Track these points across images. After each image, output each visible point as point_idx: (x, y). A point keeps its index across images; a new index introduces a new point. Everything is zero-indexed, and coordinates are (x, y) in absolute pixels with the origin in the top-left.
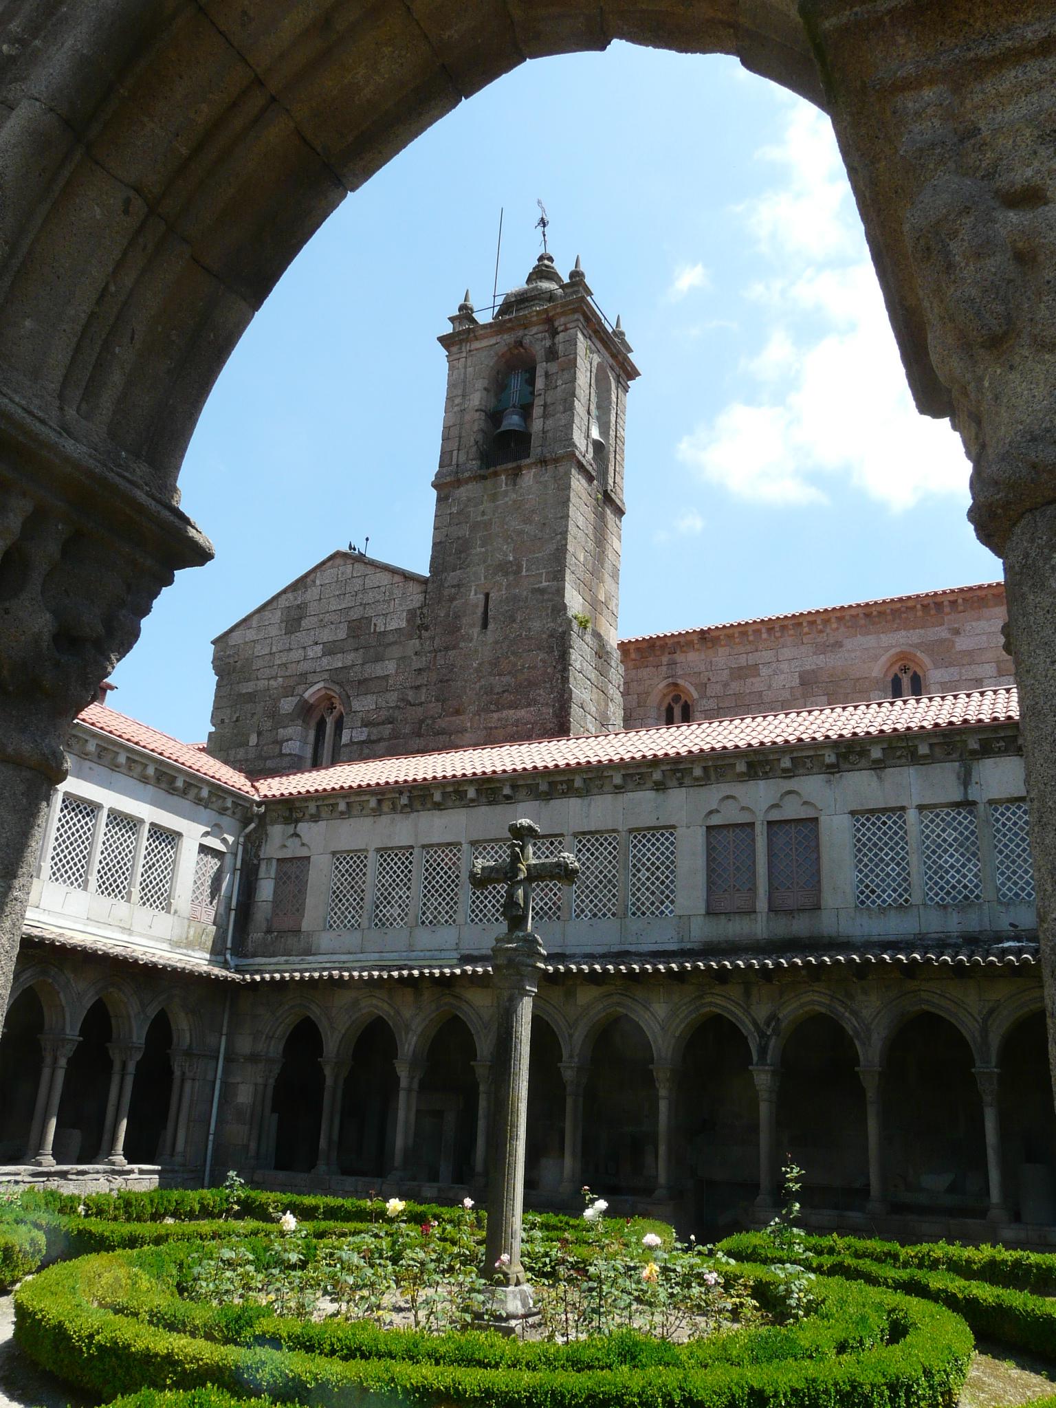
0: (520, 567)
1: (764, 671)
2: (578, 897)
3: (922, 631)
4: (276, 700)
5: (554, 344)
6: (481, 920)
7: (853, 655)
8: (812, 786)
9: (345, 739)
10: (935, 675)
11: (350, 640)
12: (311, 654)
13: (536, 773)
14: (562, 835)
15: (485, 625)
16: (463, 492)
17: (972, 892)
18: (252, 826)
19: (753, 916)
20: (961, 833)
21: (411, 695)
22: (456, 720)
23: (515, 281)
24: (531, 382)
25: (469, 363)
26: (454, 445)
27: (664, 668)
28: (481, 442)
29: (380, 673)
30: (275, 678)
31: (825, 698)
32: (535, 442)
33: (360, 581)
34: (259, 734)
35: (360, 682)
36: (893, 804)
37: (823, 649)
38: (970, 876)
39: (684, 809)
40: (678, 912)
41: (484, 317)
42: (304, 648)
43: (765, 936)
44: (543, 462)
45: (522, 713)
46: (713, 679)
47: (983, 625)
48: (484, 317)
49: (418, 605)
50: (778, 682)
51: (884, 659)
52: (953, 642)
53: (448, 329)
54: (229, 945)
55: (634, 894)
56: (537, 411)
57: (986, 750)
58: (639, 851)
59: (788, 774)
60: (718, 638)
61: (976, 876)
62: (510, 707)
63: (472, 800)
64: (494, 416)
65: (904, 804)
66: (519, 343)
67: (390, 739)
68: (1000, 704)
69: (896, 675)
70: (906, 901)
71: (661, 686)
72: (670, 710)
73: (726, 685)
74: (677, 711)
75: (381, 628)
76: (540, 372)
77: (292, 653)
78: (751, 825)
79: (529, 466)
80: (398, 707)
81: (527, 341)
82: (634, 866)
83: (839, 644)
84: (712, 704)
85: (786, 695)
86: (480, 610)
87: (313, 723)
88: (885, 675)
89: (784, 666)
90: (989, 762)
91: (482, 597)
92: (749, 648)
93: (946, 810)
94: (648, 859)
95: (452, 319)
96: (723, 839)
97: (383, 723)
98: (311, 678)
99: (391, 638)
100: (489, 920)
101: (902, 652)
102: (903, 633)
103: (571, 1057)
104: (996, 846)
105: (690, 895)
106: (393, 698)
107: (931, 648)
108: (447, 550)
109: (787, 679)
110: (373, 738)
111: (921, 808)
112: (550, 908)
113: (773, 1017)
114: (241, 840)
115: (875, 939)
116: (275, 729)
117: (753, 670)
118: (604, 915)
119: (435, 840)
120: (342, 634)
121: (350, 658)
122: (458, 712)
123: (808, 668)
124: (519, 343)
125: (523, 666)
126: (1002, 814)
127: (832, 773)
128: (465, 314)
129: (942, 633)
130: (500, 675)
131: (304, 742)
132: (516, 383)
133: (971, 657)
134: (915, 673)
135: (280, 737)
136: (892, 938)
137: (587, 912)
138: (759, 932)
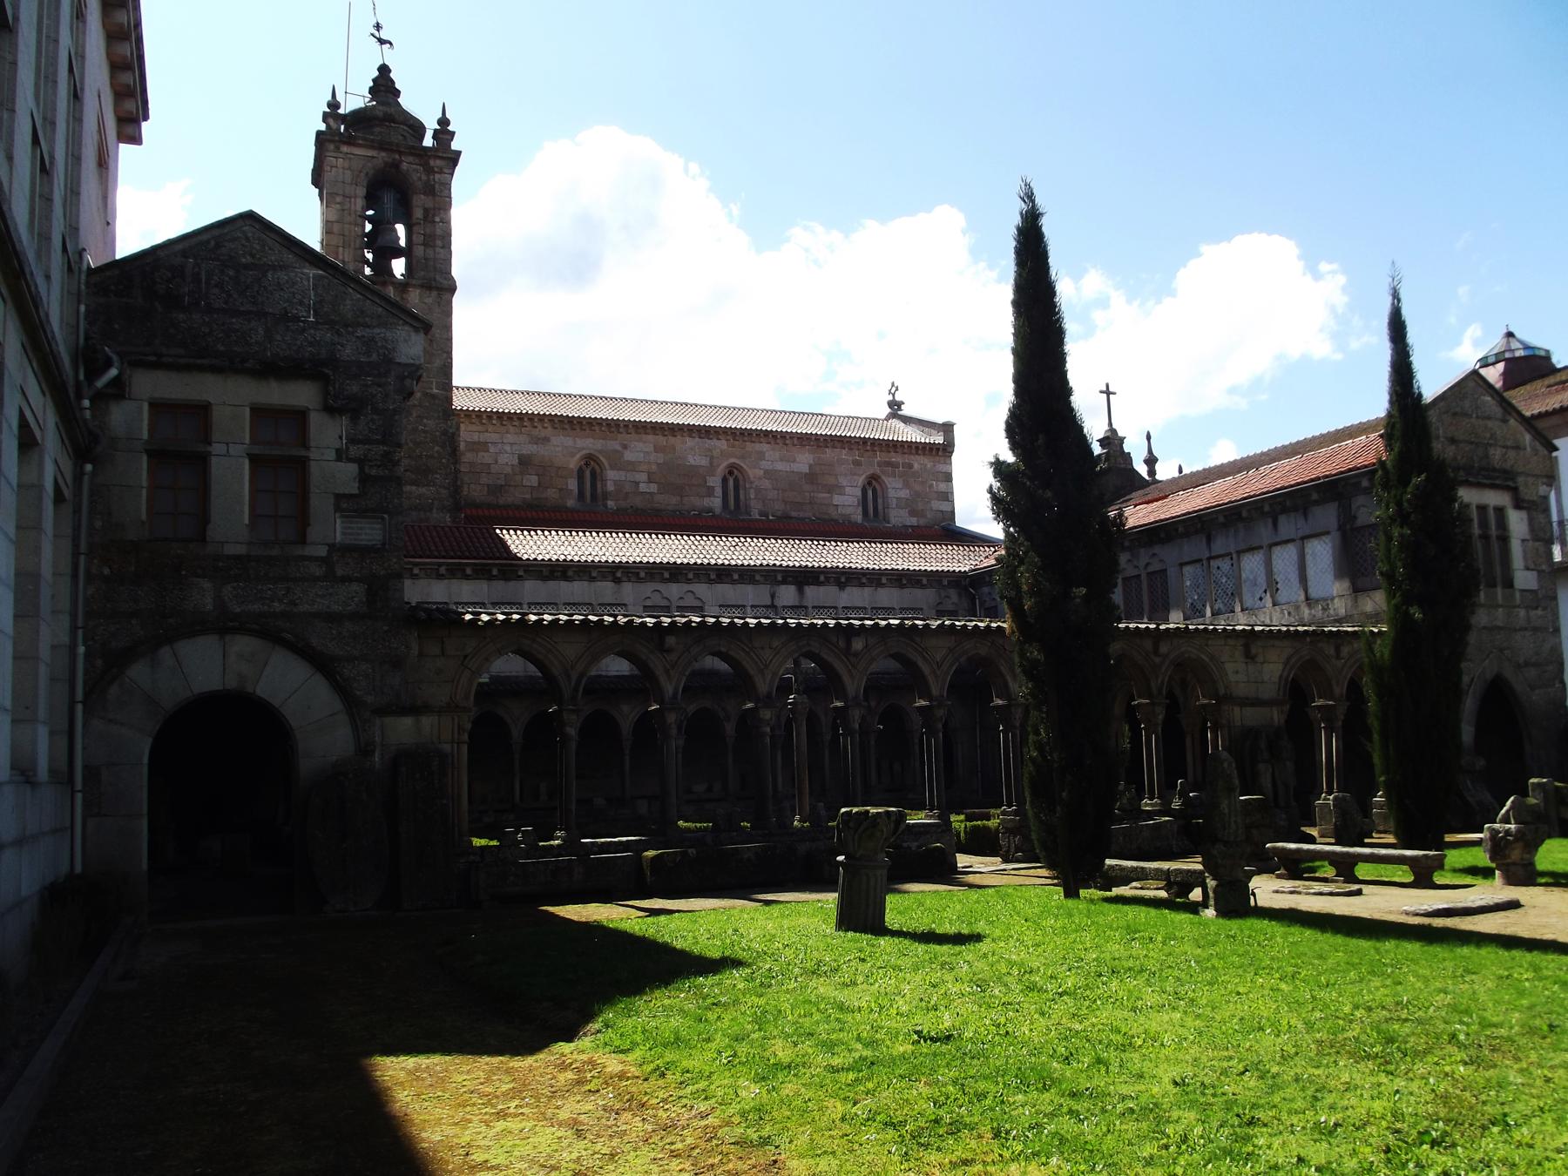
37: (537, 441)
45: (423, 490)
50: (503, 459)
57: (784, 582)
59: (688, 581)
66: (396, 165)
81: (404, 166)
92: (480, 428)
129: (614, 445)
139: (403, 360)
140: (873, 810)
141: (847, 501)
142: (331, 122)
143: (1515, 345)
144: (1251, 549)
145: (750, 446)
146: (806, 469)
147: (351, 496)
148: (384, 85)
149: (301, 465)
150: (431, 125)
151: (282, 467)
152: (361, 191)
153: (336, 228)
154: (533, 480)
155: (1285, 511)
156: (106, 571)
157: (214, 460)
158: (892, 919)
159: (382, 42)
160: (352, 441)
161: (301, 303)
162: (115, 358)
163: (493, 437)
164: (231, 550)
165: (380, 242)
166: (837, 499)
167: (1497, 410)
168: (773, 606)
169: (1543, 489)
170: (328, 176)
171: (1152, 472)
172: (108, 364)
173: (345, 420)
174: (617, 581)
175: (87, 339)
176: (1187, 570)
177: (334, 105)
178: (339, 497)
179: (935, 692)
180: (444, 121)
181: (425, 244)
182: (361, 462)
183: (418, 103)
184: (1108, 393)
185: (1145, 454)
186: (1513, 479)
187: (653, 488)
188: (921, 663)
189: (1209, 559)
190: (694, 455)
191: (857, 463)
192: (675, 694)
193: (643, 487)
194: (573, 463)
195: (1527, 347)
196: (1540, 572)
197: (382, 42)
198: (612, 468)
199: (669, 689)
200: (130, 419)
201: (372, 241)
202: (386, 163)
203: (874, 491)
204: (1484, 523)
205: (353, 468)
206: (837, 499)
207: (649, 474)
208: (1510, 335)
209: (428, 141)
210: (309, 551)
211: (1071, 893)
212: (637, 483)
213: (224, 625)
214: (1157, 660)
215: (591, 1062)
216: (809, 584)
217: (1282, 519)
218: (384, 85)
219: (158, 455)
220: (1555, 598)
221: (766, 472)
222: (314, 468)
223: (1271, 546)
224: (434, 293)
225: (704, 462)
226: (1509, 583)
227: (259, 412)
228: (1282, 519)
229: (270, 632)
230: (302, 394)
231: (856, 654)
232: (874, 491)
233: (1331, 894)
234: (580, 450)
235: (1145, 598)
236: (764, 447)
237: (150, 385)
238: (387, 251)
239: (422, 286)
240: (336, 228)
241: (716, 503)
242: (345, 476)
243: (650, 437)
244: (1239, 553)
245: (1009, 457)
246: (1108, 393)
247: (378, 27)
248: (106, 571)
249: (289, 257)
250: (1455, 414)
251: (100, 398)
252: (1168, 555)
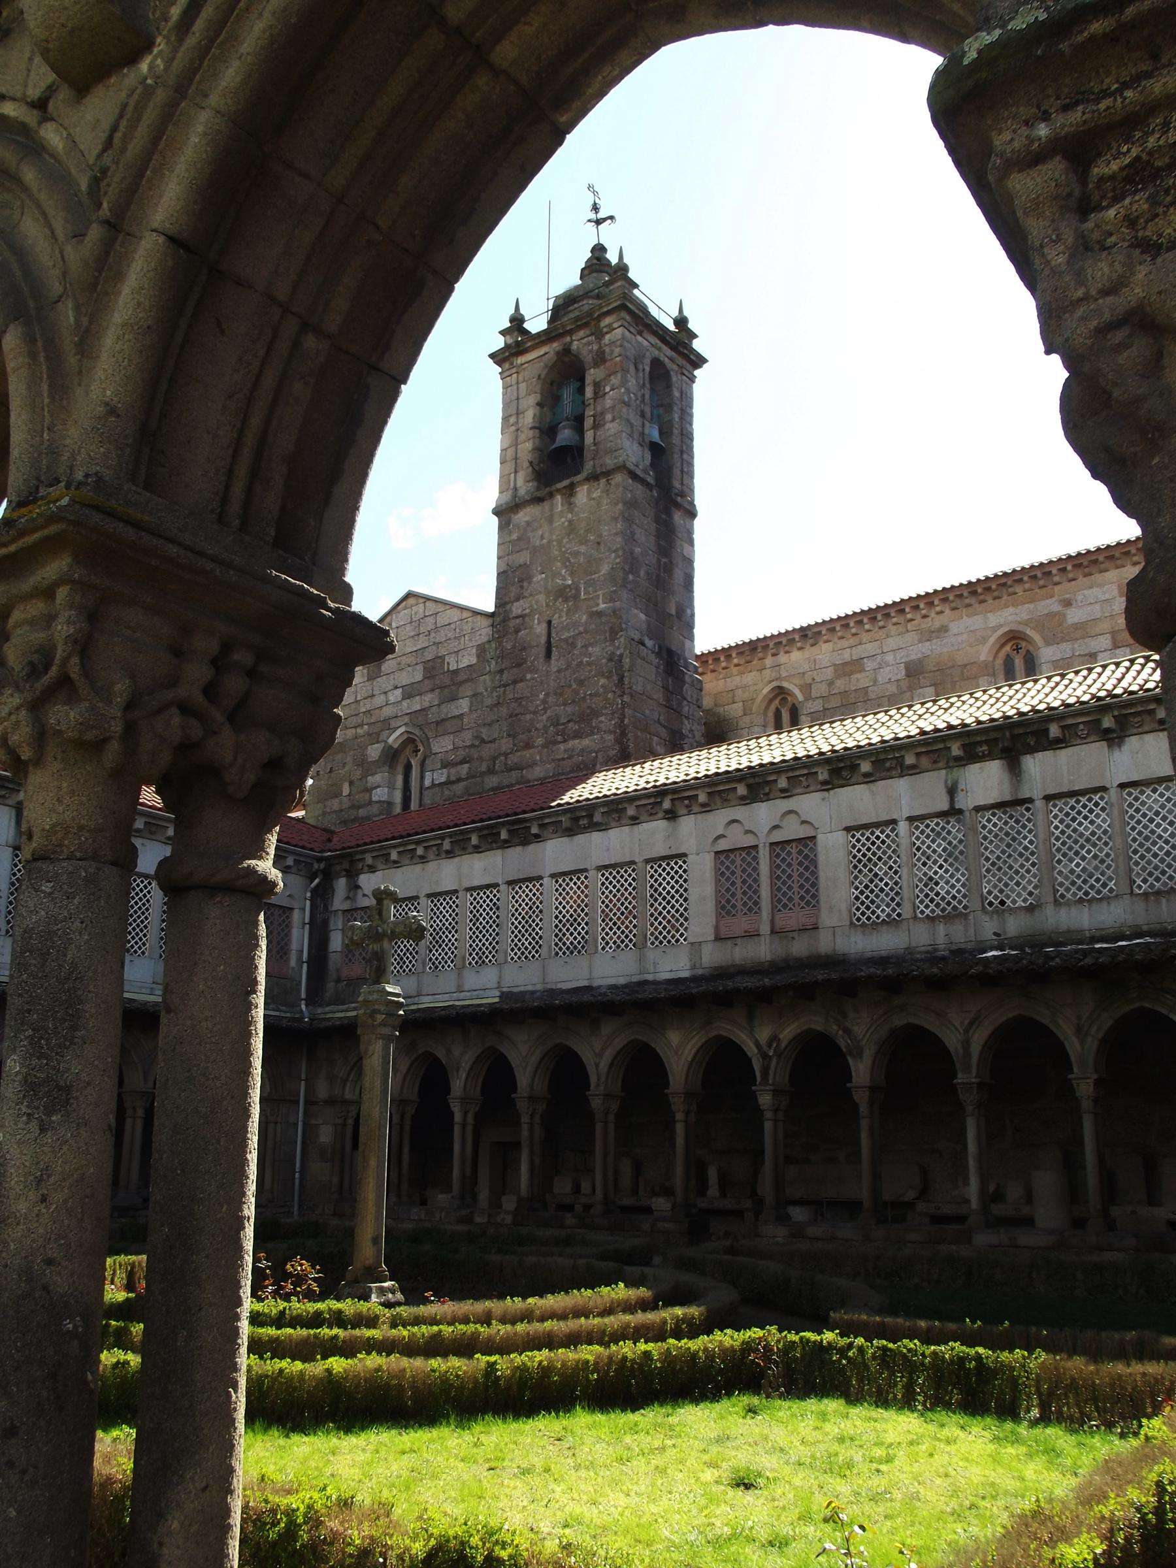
0: (578, 590)
1: (869, 665)
2: (603, 929)
3: (1031, 606)
4: (363, 748)
5: (600, 347)
6: (519, 958)
7: (959, 639)
8: (811, 805)
9: (427, 783)
10: (1047, 654)
11: (426, 681)
12: (392, 699)
13: (660, 792)
14: (585, 870)
15: (548, 654)
16: (522, 516)
17: (960, 902)
18: (317, 881)
19: (756, 939)
20: (950, 843)
21: (485, 733)
22: (527, 754)
23: (569, 278)
24: (581, 390)
25: (521, 378)
26: (510, 467)
27: (768, 672)
28: (536, 462)
29: (456, 713)
30: (361, 725)
31: (931, 690)
32: (587, 454)
33: (431, 620)
34: (351, 783)
35: (438, 723)
36: (884, 817)
37: (929, 635)
38: (958, 886)
39: (694, 833)
40: (691, 939)
41: (536, 324)
42: (385, 693)
43: (768, 958)
44: (594, 477)
45: (586, 742)
46: (817, 679)
47: (1096, 593)
48: (536, 324)
49: (486, 640)
50: (885, 675)
51: (992, 640)
52: (1064, 615)
53: (499, 343)
54: (303, 995)
55: (652, 925)
56: (588, 422)
58: (656, 881)
59: (786, 793)
60: (820, 633)
61: (963, 885)
62: (575, 737)
63: (505, 841)
64: (547, 430)
65: (895, 817)
66: (567, 350)
67: (467, 779)
68: (1140, 674)
69: (1008, 655)
70: (899, 915)
71: (766, 690)
72: (778, 715)
73: (831, 684)
74: (786, 716)
75: (453, 667)
76: (589, 379)
77: (375, 699)
78: (755, 847)
79: (581, 483)
80: (473, 746)
81: (575, 346)
82: (652, 896)
84: (817, 706)
85: (892, 689)
86: (543, 639)
87: (400, 768)
88: (995, 657)
89: (889, 658)
90: (975, 768)
91: (544, 625)
92: (852, 641)
93: (936, 820)
94: (664, 889)
95: (503, 333)
96: (732, 862)
97: (461, 763)
98: (393, 724)
99: (463, 676)
100: (526, 958)
101: (1011, 631)
102: (1011, 609)
103: (598, 1085)
104: (983, 854)
105: (701, 923)
106: (467, 737)
107: (1039, 624)
108: (510, 581)
109: (892, 673)
110: (453, 778)
111: (911, 819)
112: (579, 943)
113: (774, 1038)
114: (309, 895)
115: (869, 955)
116: (364, 777)
117: (856, 665)
118: (627, 946)
119: (476, 883)
120: (419, 677)
121: (428, 699)
122: (528, 746)
123: (914, 657)
124: (567, 350)
125: (585, 693)
126: (989, 821)
127: (827, 790)
128: (517, 321)
129: (1053, 605)
130: (565, 704)
131: (391, 787)
132: (568, 394)
133: (1083, 630)
134: (1028, 651)
135: (369, 785)
136: (883, 953)
137: (611, 944)
138: (763, 954)
147: (1161, 780)
163: (870, 648)
174: (671, 816)
198: (1048, 643)
202: (557, 353)
216: (1032, 750)
234: (995, 629)
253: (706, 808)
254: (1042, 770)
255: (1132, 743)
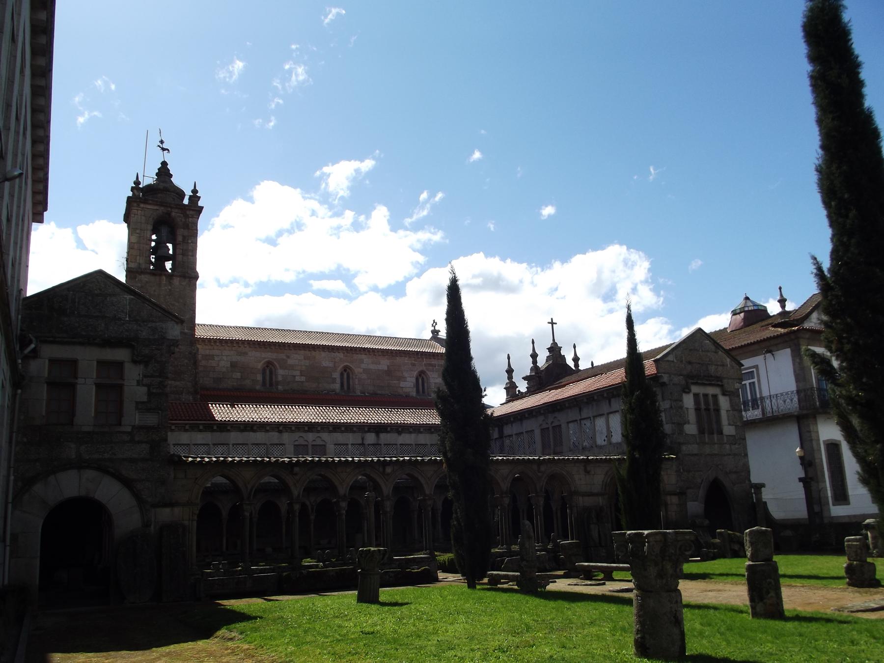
1: (216, 359)
8: (325, 436)
45: (178, 383)
50: (222, 363)
57: (369, 431)
59: (318, 432)
66: (169, 214)
81: (173, 214)
83: (245, 354)
129: (282, 356)
139: (170, 337)
140: (372, 549)
141: (408, 385)
142: (135, 191)
143: (749, 304)
144: (601, 415)
145: (356, 356)
146: (386, 368)
148: (164, 172)
149: (120, 388)
150: (188, 193)
151: (110, 388)
152: (150, 227)
153: (136, 246)
154: (238, 375)
155: (614, 396)
156: (25, 440)
157: (78, 386)
158: (382, 598)
159: (163, 149)
160: (145, 376)
161: (123, 311)
162: (34, 339)
164: (86, 429)
165: (160, 253)
166: (402, 384)
167: (713, 348)
168: (363, 444)
169: (737, 385)
170: (133, 219)
171: (577, 365)
172: (31, 342)
173: (142, 367)
174: (280, 432)
175: (21, 330)
176: (571, 425)
177: (137, 183)
178: (137, 403)
179: (427, 492)
180: (195, 191)
181: (183, 254)
182: (148, 386)
183: (182, 180)
184: (552, 323)
185: (572, 355)
186: (721, 381)
187: (303, 379)
188: (420, 478)
189: (581, 420)
190: (325, 361)
191: (414, 365)
192: (299, 495)
193: (298, 379)
194: (260, 366)
195: (755, 305)
196: (736, 426)
197: (163, 149)
199: (295, 493)
200: (39, 368)
201: (155, 251)
203: (423, 379)
204: (707, 403)
205: (145, 389)
206: (402, 384)
207: (301, 371)
208: (747, 298)
209: (186, 201)
210: (122, 429)
211: (472, 585)
212: (294, 376)
213: (80, 465)
214: (540, 474)
215: (238, 647)
217: (613, 400)
218: (164, 172)
219: (52, 384)
220: (745, 439)
221: (364, 370)
222: (126, 389)
223: (608, 414)
224: (187, 280)
225: (331, 365)
226: (720, 432)
227: (100, 363)
228: (613, 400)
229: (102, 468)
230: (122, 354)
231: (388, 474)
232: (423, 379)
233: (591, 585)
235: (552, 440)
236: (363, 356)
237: (50, 351)
238: (162, 259)
239: (180, 276)
240: (136, 246)
241: (337, 386)
242: (141, 393)
243: (302, 352)
244: (594, 417)
245: (444, 388)
246: (552, 323)
247: (162, 142)
248: (25, 440)
249: (118, 290)
250: (691, 350)
251: (26, 358)
252: (562, 418)
253: (292, 431)
254: (384, 437)
255: (403, 435)
